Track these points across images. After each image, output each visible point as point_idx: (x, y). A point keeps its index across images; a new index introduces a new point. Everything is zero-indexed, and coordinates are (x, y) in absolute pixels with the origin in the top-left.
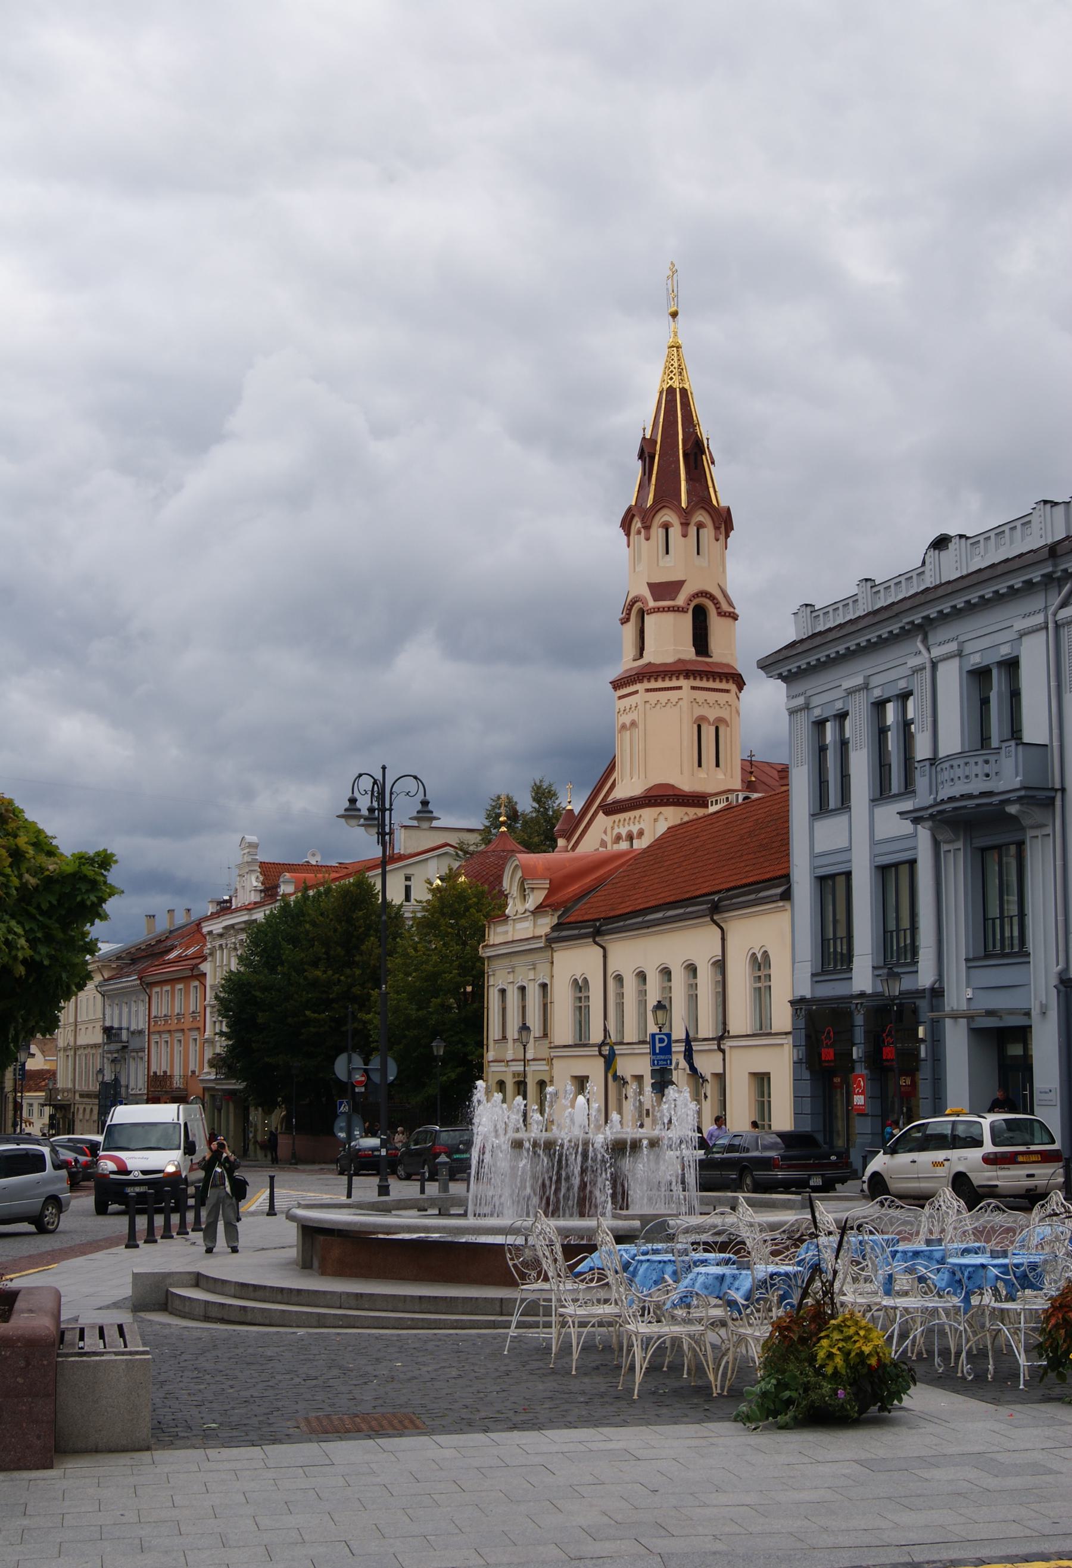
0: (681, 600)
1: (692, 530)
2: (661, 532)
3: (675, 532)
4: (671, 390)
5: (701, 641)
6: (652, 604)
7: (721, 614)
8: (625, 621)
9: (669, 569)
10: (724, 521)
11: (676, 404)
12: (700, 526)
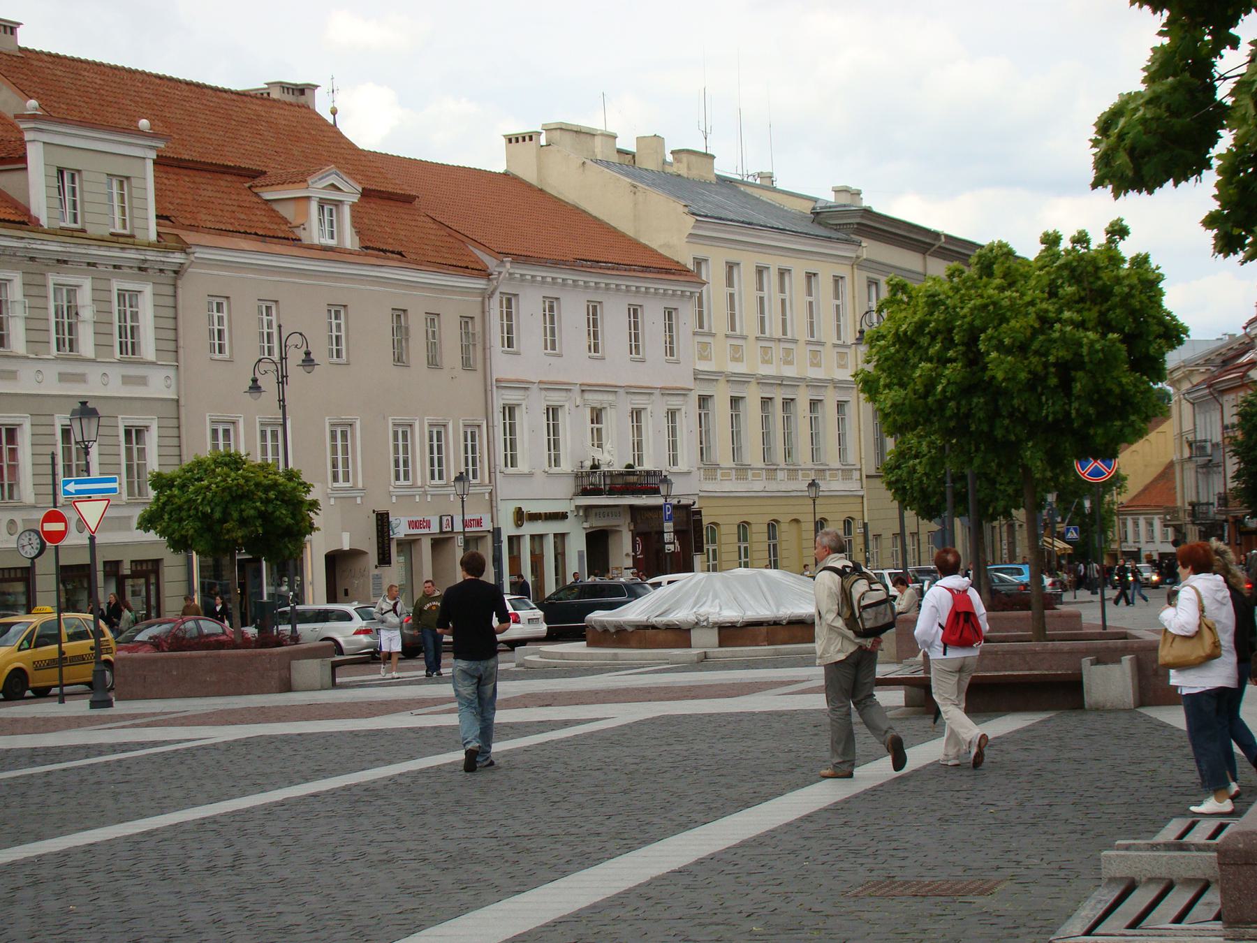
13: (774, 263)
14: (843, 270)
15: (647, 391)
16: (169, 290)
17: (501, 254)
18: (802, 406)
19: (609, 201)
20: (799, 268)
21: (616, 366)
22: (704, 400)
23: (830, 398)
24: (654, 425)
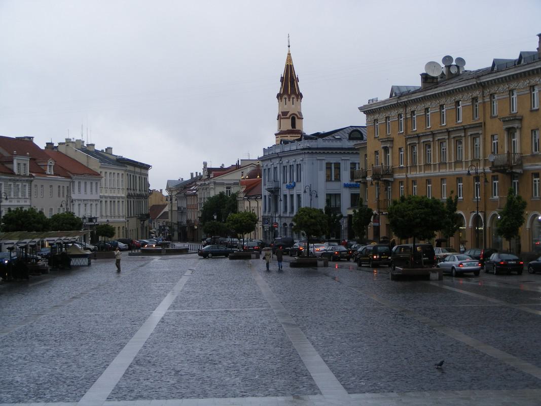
0: (288, 116)
2: (284, 100)
3: (287, 100)
4: (287, 66)
5: (293, 125)
6: (282, 117)
7: (298, 118)
8: (278, 119)
9: (286, 109)
10: (300, 96)
11: (289, 69)
12: (293, 98)
13: (112, 171)
14: (123, 172)
15: (87, 200)
17: (72, 174)
18: (116, 202)
19: (82, 158)
20: (116, 172)
21: (89, 196)
22: (101, 201)
23: (121, 200)
24: (94, 206)
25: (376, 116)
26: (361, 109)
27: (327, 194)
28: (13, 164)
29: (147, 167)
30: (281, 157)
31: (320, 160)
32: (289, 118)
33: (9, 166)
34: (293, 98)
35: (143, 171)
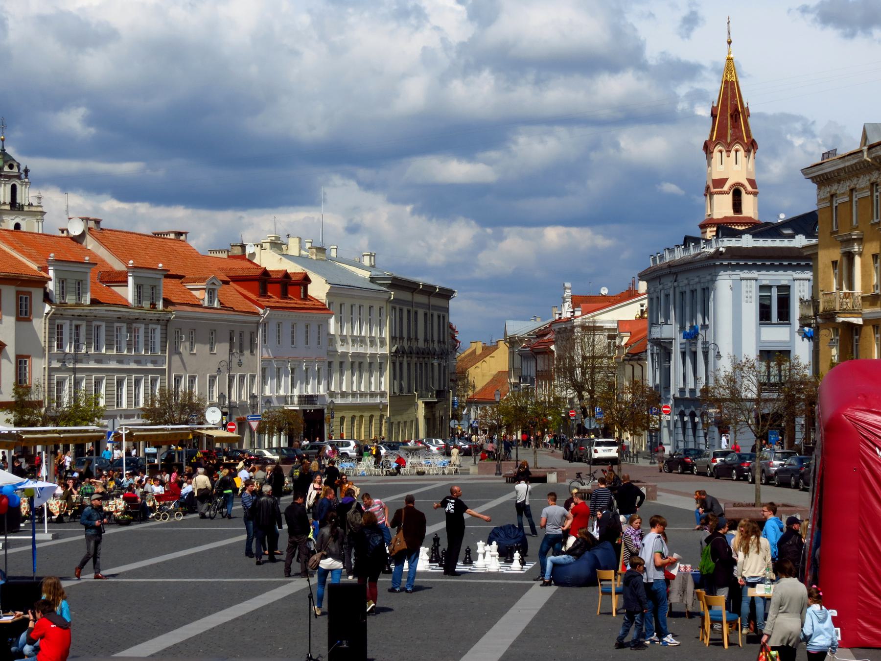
1: (733, 153)
3: (724, 154)
5: (737, 206)
7: (748, 193)
11: (730, 90)
12: (737, 151)
16: (164, 327)
25: (834, 188)
26: (806, 171)
27: (761, 351)
28: (127, 286)
29: (447, 294)
30: (676, 274)
31: (747, 279)
32: (728, 193)
33: (118, 290)
34: (737, 151)
35: (435, 301)
